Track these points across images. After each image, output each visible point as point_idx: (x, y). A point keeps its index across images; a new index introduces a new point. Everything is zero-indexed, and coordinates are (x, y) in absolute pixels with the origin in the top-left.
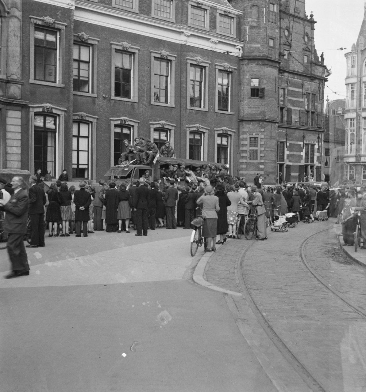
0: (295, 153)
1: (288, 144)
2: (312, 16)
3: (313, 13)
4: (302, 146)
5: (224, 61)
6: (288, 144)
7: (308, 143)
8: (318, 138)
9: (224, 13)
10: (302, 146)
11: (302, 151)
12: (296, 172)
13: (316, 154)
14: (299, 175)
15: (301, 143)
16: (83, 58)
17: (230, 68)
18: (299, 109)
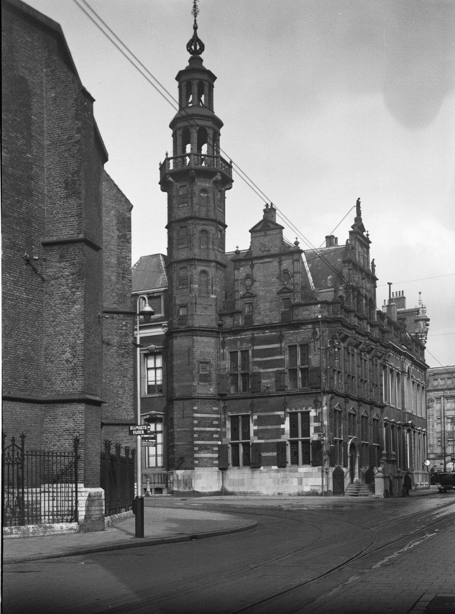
0: (269, 427)
1: (255, 417)
7: (294, 411)
13: (313, 425)
14: (278, 454)
15: (281, 413)
18: (275, 369)
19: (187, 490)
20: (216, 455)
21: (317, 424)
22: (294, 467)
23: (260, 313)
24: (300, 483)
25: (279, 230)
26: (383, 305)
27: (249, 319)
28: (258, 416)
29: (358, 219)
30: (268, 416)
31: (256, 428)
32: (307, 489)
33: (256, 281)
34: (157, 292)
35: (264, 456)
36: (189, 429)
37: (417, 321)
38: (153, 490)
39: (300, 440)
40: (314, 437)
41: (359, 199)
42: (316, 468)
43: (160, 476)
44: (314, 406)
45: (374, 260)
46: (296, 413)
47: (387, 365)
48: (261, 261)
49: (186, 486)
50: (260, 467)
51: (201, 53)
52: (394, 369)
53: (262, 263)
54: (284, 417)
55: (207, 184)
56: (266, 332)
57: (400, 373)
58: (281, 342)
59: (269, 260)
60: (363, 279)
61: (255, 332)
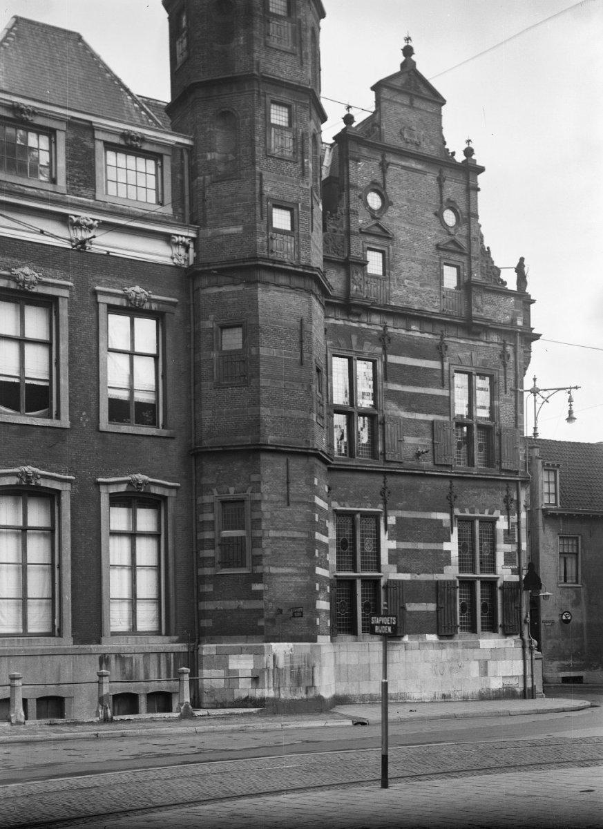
0: (421, 546)
1: (392, 520)
2: (469, 152)
3: (471, 145)
4: (446, 524)
5: (130, 282)
7: (468, 514)
8: (507, 500)
9: (122, 143)
11: (449, 540)
12: (427, 602)
13: (503, 548)
14: (438, 609)
15: (444, 517)
16: (29, 334)
17: (150, 300)
18: (431, 417)
19: (301, 695)
21: (509, 548)
22: (470, 638)
23: (400, 282)
24: (484, 672)
28: (398, 519)
30: (419, 520)
31: (393, 545)
32: (496, 684)
33: (391, 204)
34: (152, 143)
35: (411, 613)
36: (303, 535)
38: (32, 706)
39: (478, 578)
40: (504, 574)
42: (508, 639)
43: (163, 657)
44: (503, 506)
46: (471, 521)
48: (403, 163)
49: (299, 685)
50: (403, 636)
53: (404, 167)
54: (449, 525)
56: (413, 327)
59: (419, 167)
61: (390, 323)
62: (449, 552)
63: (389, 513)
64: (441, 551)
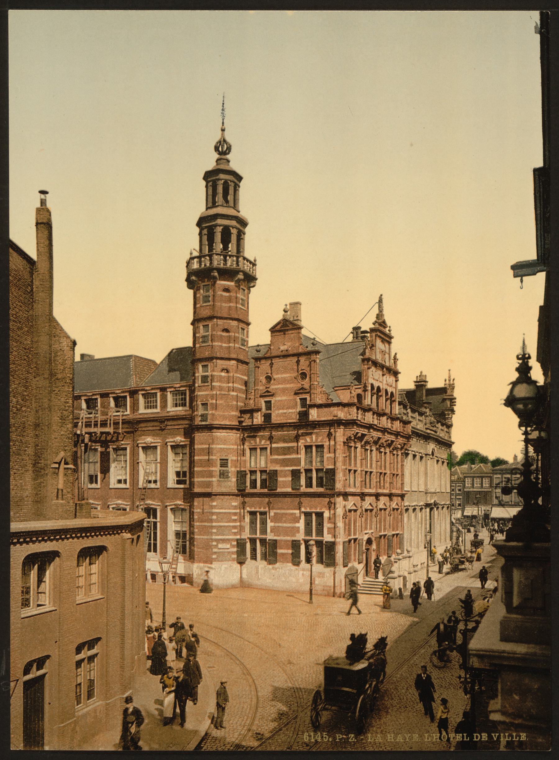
1: (272, 514)
6: (272, 514)
7: (308, 510)
10: (298, 515)
11: (299, 522)
12: (288, 549)
15: (297, 512)
18: (291, 468)
20: (235, 550)
25: (296, 331)
26: (415, 380)
27: (268, 417)
28: (275, 513)
29: (380, 315)
37: (444, 400)
40: (327, 537)
41: (381, 295)
45: (396, 354)
47: (409, 452)
51: (229, 153)
52: (417, 454)
55: (231, 284)
57: (424, 455)
58: (297, 442)
60: (383, 375)
62: (299, 528)
63: (271, 511)
64: (295, 527)
